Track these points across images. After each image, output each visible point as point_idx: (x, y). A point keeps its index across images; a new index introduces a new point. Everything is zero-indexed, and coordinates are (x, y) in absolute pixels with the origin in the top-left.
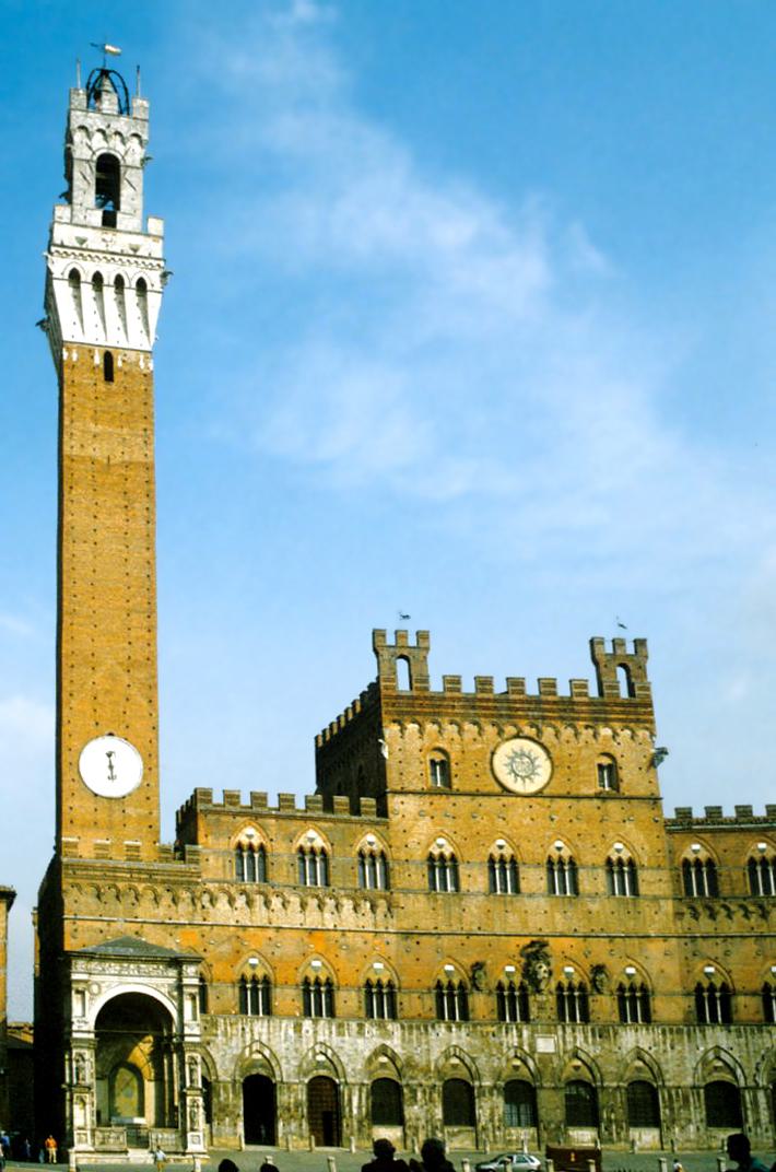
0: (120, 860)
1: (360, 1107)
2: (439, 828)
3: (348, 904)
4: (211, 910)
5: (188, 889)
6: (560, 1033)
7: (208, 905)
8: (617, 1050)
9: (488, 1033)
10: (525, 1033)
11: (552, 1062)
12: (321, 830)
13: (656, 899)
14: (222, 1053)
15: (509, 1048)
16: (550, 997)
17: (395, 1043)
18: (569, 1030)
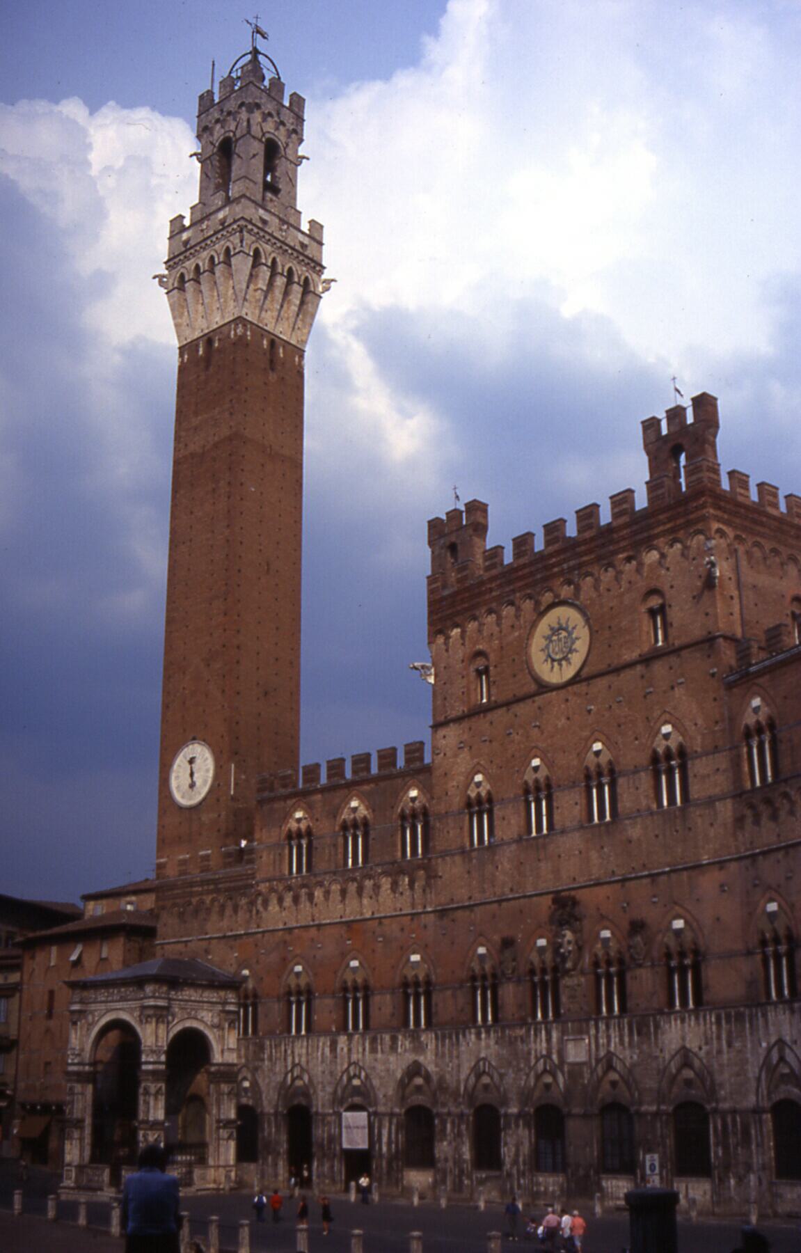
0: (195, 874)
1: (389, 1143)
2: (476, 761)
3: (386, 883)
4: (264, 915)
5: (244, 895)
6: (593, 1032)
7: (261, 908)
8: (658, 1053)
9: (516, 1038)
10: (555, 1035)
11: (583, 1078)
12: (361, 797)
13: (711, 801)
14: (267, 1080)
15: (537, 1060)
16: (583, 980)
17: (428, 1060)
18: (602, 1026)
